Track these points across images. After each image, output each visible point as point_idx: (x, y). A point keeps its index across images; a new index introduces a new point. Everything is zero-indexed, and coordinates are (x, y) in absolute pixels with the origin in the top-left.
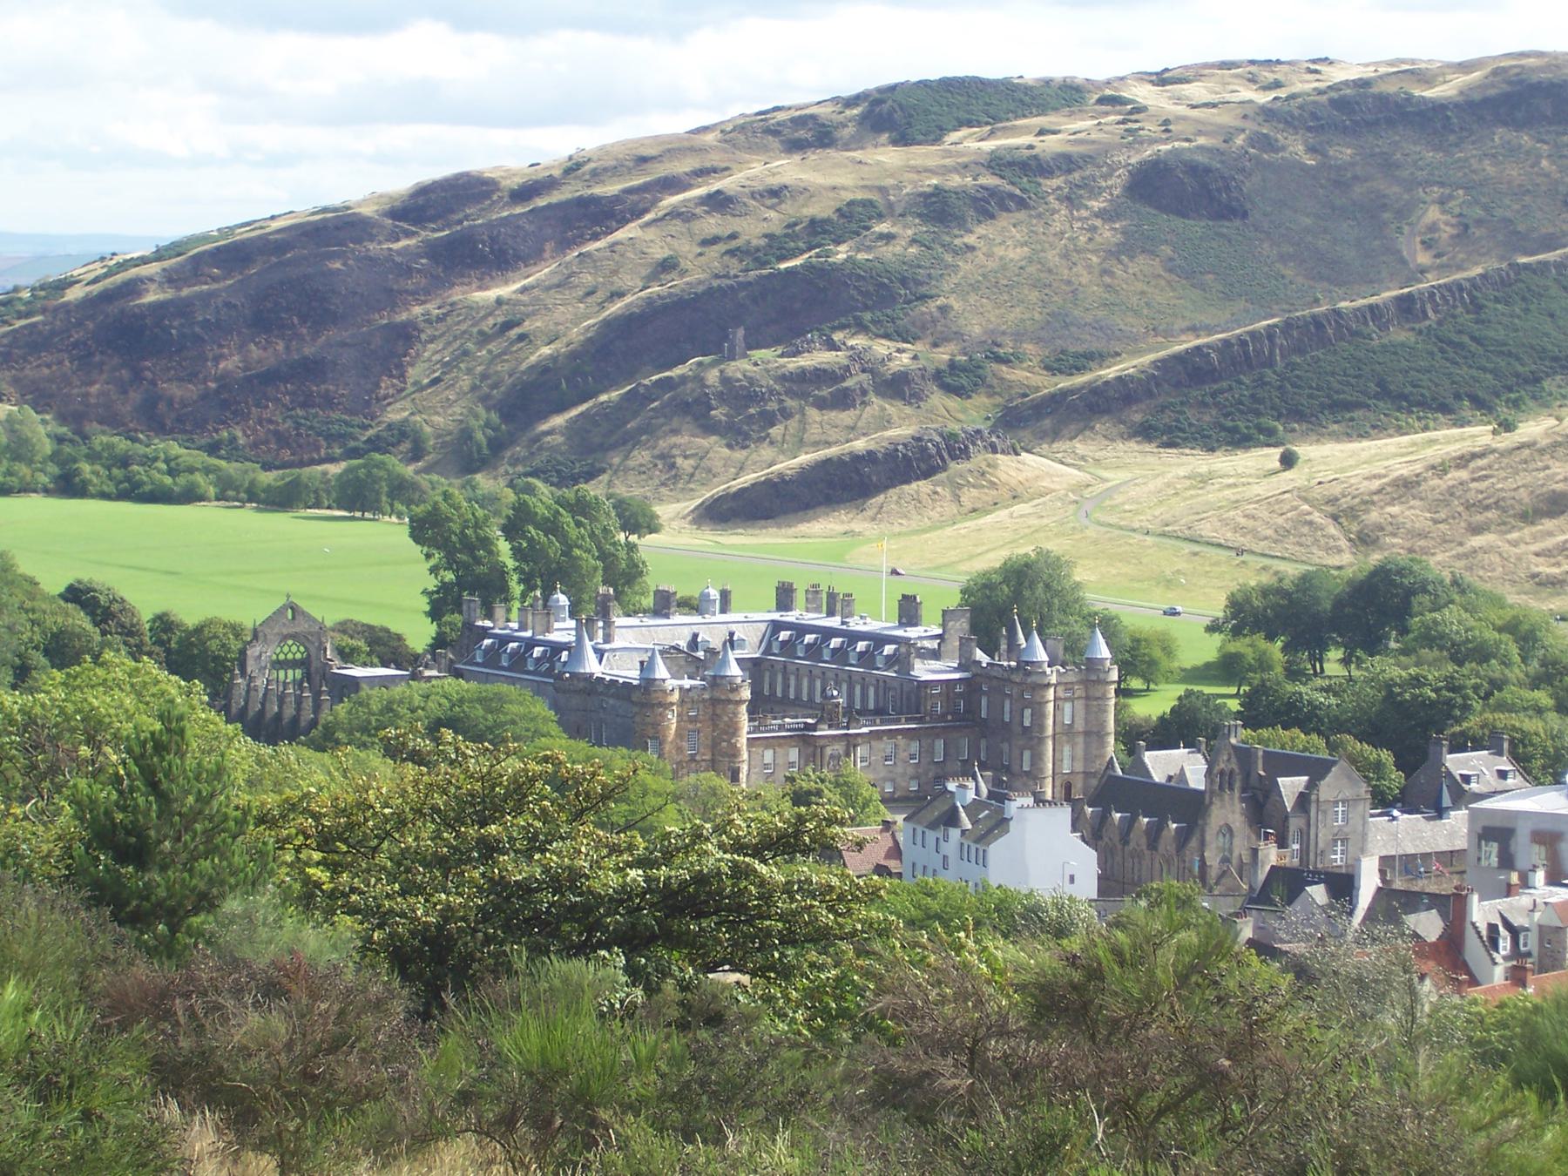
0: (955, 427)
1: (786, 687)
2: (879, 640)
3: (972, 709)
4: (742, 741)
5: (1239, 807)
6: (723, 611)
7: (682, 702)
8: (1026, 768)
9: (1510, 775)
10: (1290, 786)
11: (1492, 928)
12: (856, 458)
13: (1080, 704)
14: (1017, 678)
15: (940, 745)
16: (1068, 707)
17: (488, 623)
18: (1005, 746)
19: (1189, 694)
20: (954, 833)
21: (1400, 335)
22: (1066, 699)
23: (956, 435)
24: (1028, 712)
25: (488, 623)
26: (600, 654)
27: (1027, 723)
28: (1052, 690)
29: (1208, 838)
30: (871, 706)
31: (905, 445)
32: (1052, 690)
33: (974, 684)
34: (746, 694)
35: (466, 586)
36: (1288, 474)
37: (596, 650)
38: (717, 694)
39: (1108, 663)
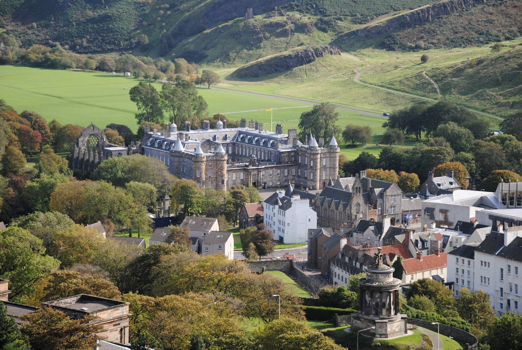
0: (318, 46)
1: (242, 151)
2: (269, 138)
3: (296, 160)
4: (225, 172)
5: (362, 197)
6: (224, 128)
7: (207, 161)
8: (311, 178)
9: (454, 183)
10: (377, 191)
11: (417, 241)
12: (286, 57)
13: (328, 159)
14: (309, 151)
15: (286, 171)
16: (324, 160)
17: (152, 133)
18: (306, 171)
19: (363, 154)
20: (277, 207)
22: (324, 158)
23: (318, 49)
24: (312, 162)
25: (152, 133)
27: (312, 165)
28: (319, 155)
29: (352, 206)
30: (266, 159)
31: (301, 53)
32: (319, 155)
33: (296, 153)
34: (226, 158)
36: (425, 65)
37: (182, 143)
38: (217, 158)
39: (337, 147)
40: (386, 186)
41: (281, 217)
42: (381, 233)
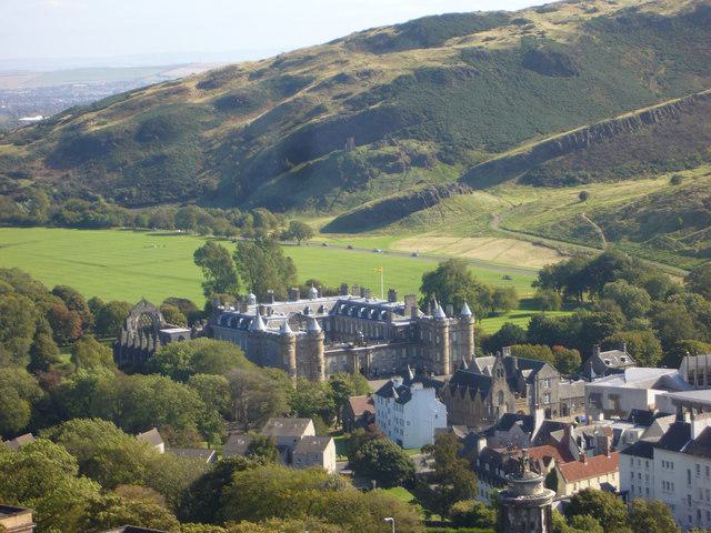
0: (443, 184)
2: (378, 308)
3: (417, 336)
4: (322, 356)
10: (526, 373)
11: (579, 439)
12: (399, 200)
15: (404, 351)
17: (223, 307)
19: (507, 325)
20: (392, 400)
21: (643, 131)
25: (223, 307)
26: (265, 321)
33: (416, 327)
34: (323, 337)
35: (221, 282)
36: (584, 204)
40: (537, 367)
41: (398, 414)
42: (532, 430)
